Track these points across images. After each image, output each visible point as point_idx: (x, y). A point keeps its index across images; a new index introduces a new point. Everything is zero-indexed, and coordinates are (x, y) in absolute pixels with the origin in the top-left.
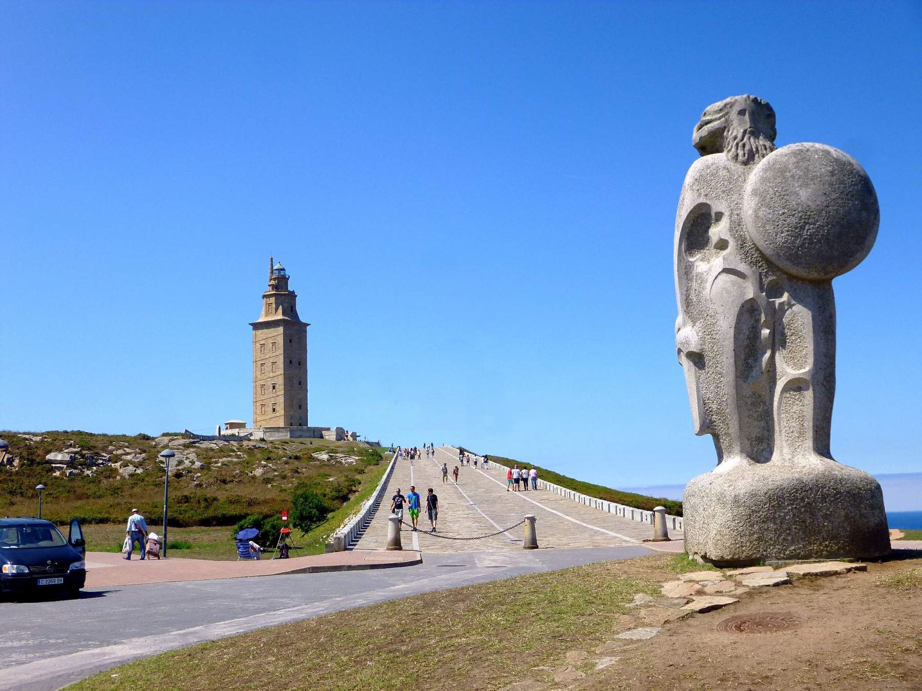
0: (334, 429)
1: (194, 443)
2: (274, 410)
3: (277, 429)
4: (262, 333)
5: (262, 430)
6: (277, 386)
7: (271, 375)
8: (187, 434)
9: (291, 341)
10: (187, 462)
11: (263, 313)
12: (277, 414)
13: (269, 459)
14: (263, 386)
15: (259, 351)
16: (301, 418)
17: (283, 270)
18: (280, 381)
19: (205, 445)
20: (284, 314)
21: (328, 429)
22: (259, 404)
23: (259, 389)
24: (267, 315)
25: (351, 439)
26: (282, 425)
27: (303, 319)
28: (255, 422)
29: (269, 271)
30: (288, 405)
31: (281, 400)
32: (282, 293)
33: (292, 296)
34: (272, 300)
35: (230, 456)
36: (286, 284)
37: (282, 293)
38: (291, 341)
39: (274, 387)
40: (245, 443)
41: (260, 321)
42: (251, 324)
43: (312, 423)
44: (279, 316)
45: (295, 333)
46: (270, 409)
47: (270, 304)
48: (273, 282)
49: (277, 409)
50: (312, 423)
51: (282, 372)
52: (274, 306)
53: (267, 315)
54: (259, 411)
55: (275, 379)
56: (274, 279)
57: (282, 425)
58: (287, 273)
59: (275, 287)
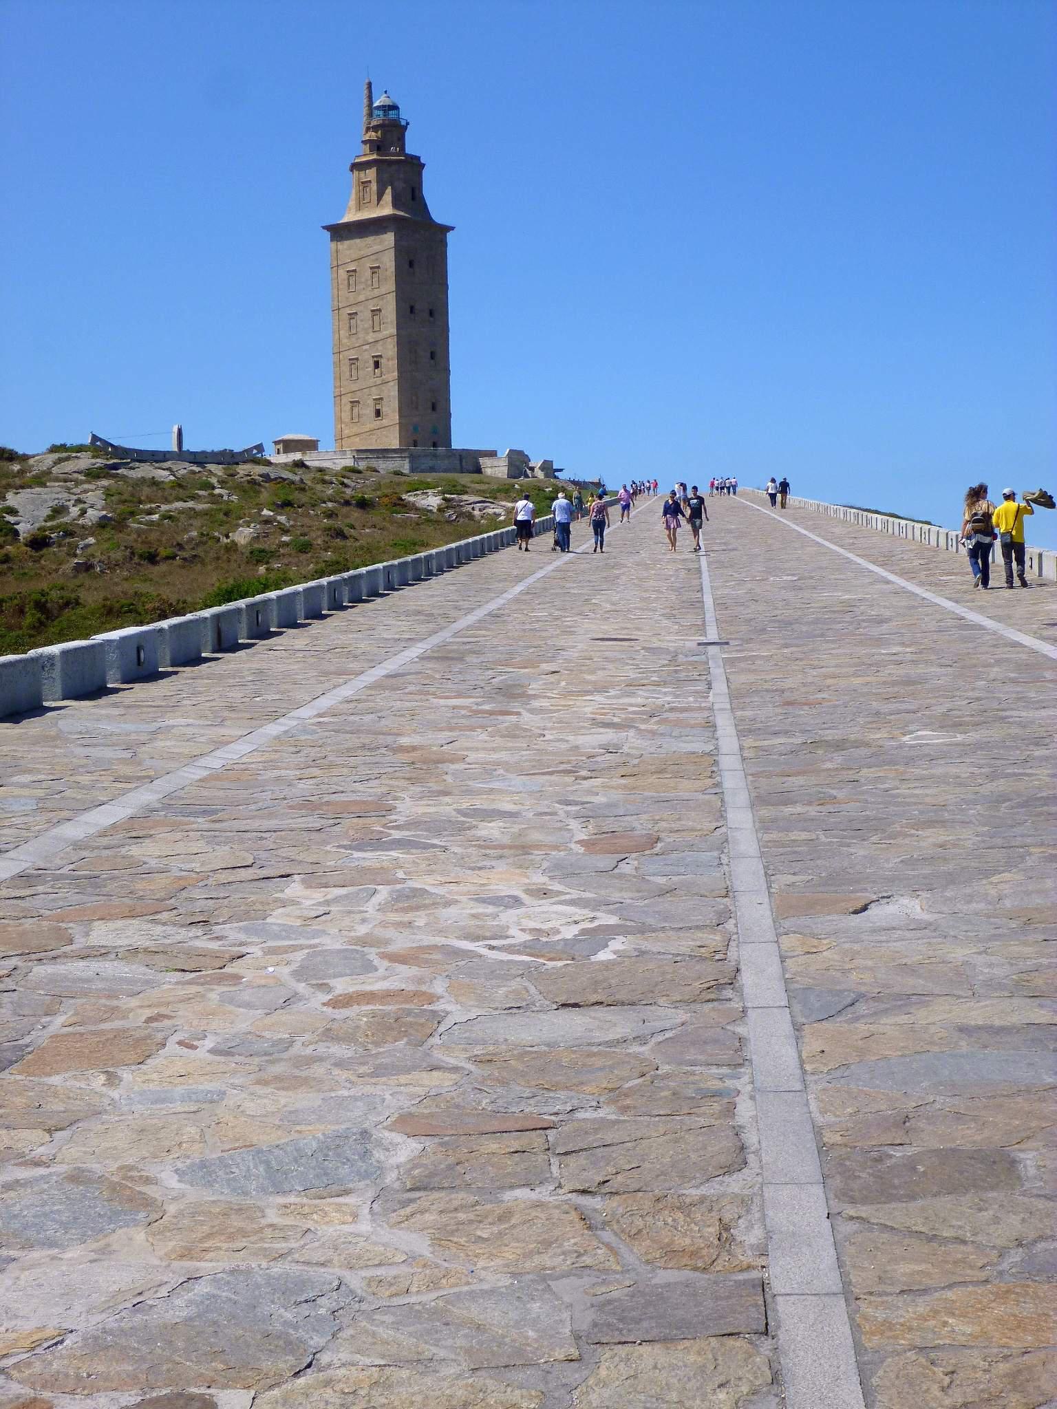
0: (504, 453)
1: (115, 467)
2: (378, 413)
3: (383, 453)
4: (352, 248)
5: (349, 455)
6: (383, 361)
7: (371, 337)
8: (99, 446)
10: (75, 511)
11: (352, 203)
12: (385, 422)
13: (287, 504)
14: (353, 361)
15: (343, 286)
16: (435, 432)
17: (394, 107)
18: (390, 351)
19: (145, 471)
20: (395, 205)
21: (492, 454)
22: (346, 400)
23: (346, 369)
24: (359, 208)
25: (540, 475)
26: (395, 444)
27: (439, 215)
28: (340, 438)
29: (365, 111)
30: (408, 403)
31: (391, 392)
32: (392, 159)
33: (415, 165)
34: (371, 174)
35: (194, 498)
36: (401, 140)
37: (392, 159)
38: (411, 264)
39: (377, 365)
40: (242, 469)
41: (345, 220)
42: (327, 228)
43: (460, 440)
44: (386, 209)
45: (420, 248)
46: (370, 412)
47: (366, 184)
48: (372, 135)
49: (384, 410)
50: (460, 440)
51: (394, 331)
52: (374, 187)
53: (359, 208)
54: (346, 416)
55: (379, 346)
56: (375, 129)
57: (395, 444)
58: (405, 115)
59: (377, 146)
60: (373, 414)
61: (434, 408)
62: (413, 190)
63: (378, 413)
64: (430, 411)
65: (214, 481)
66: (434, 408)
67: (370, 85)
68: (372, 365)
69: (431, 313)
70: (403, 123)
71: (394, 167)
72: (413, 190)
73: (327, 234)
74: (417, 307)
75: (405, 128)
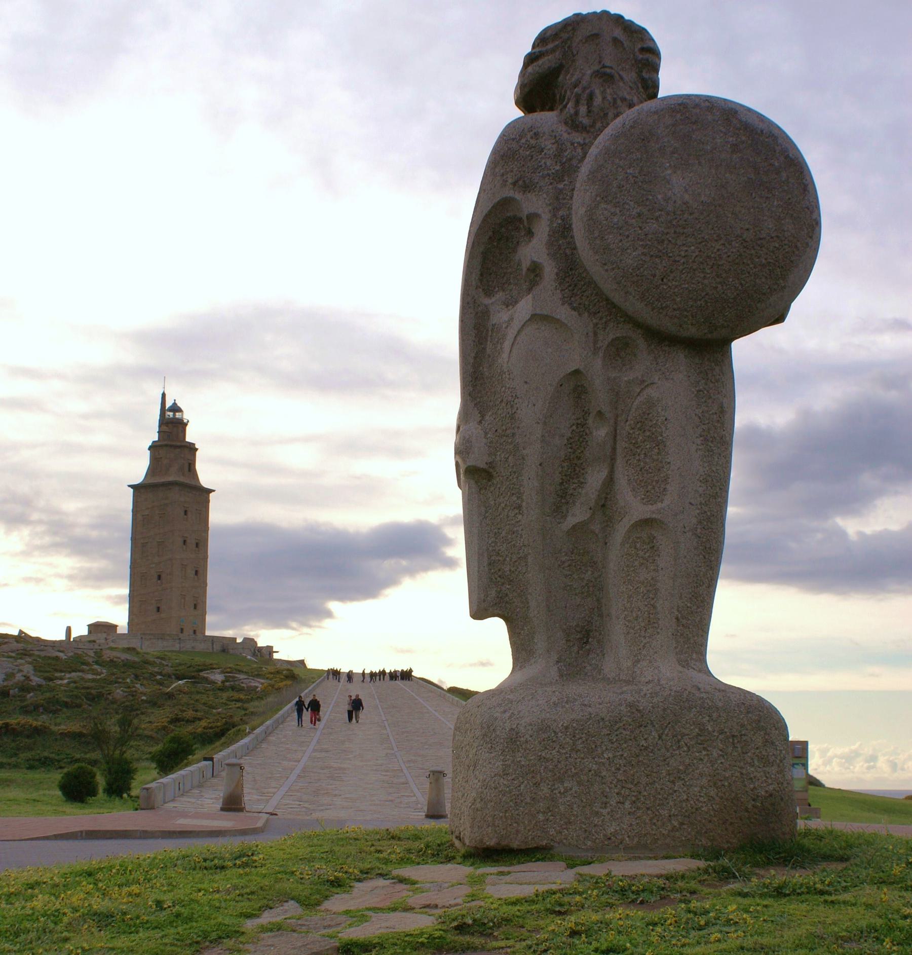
2: (158, 609)
6: (163, 576)
9: (186, 513)
12: (163, 615)
38: (186, 513)
39: (159, 577)
44: (171, 479)
60: (155, 610)
61: (195, 607)
62: (190, 464)
63: (158, 609)
64: (192, 608)
65: (91, 660)
66: (195, 607)
67: (164, 395)
68: (156, 576)
69: (197, 545)
70: (185, 421)
71: (178, 450)
72: (190, 464)
73: (132, 490)
74: (188, 541)
75: (186, 425)
